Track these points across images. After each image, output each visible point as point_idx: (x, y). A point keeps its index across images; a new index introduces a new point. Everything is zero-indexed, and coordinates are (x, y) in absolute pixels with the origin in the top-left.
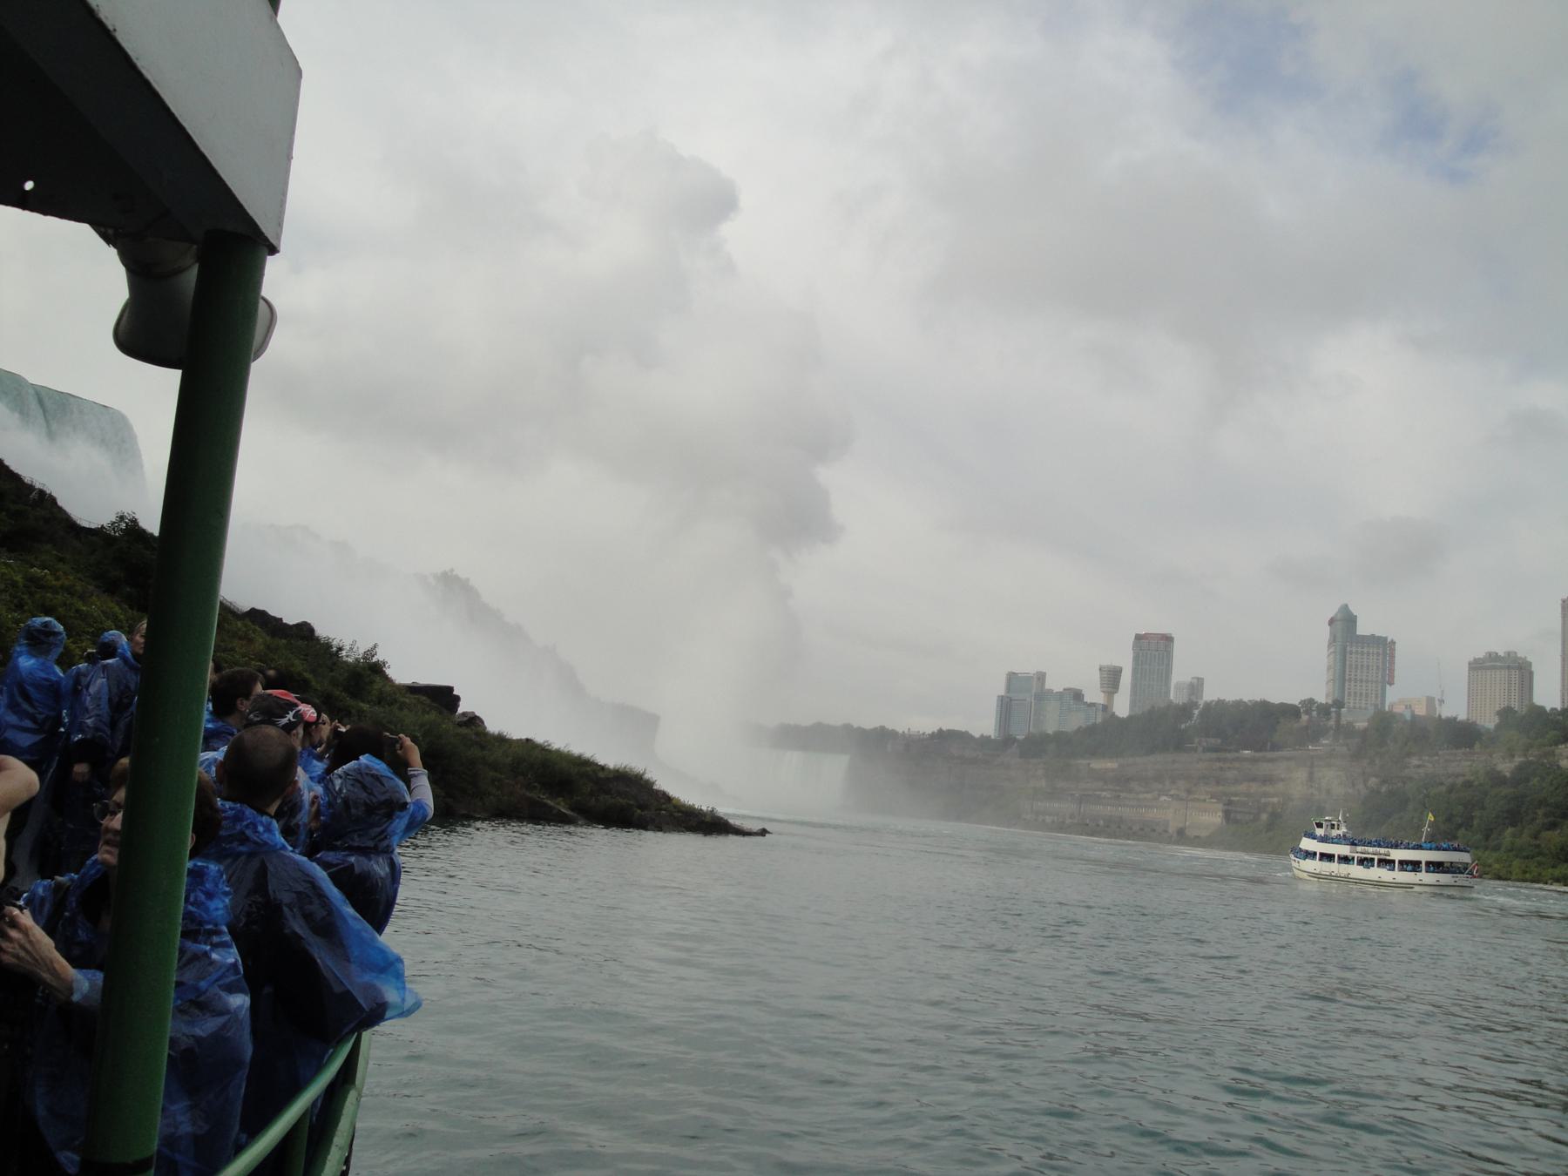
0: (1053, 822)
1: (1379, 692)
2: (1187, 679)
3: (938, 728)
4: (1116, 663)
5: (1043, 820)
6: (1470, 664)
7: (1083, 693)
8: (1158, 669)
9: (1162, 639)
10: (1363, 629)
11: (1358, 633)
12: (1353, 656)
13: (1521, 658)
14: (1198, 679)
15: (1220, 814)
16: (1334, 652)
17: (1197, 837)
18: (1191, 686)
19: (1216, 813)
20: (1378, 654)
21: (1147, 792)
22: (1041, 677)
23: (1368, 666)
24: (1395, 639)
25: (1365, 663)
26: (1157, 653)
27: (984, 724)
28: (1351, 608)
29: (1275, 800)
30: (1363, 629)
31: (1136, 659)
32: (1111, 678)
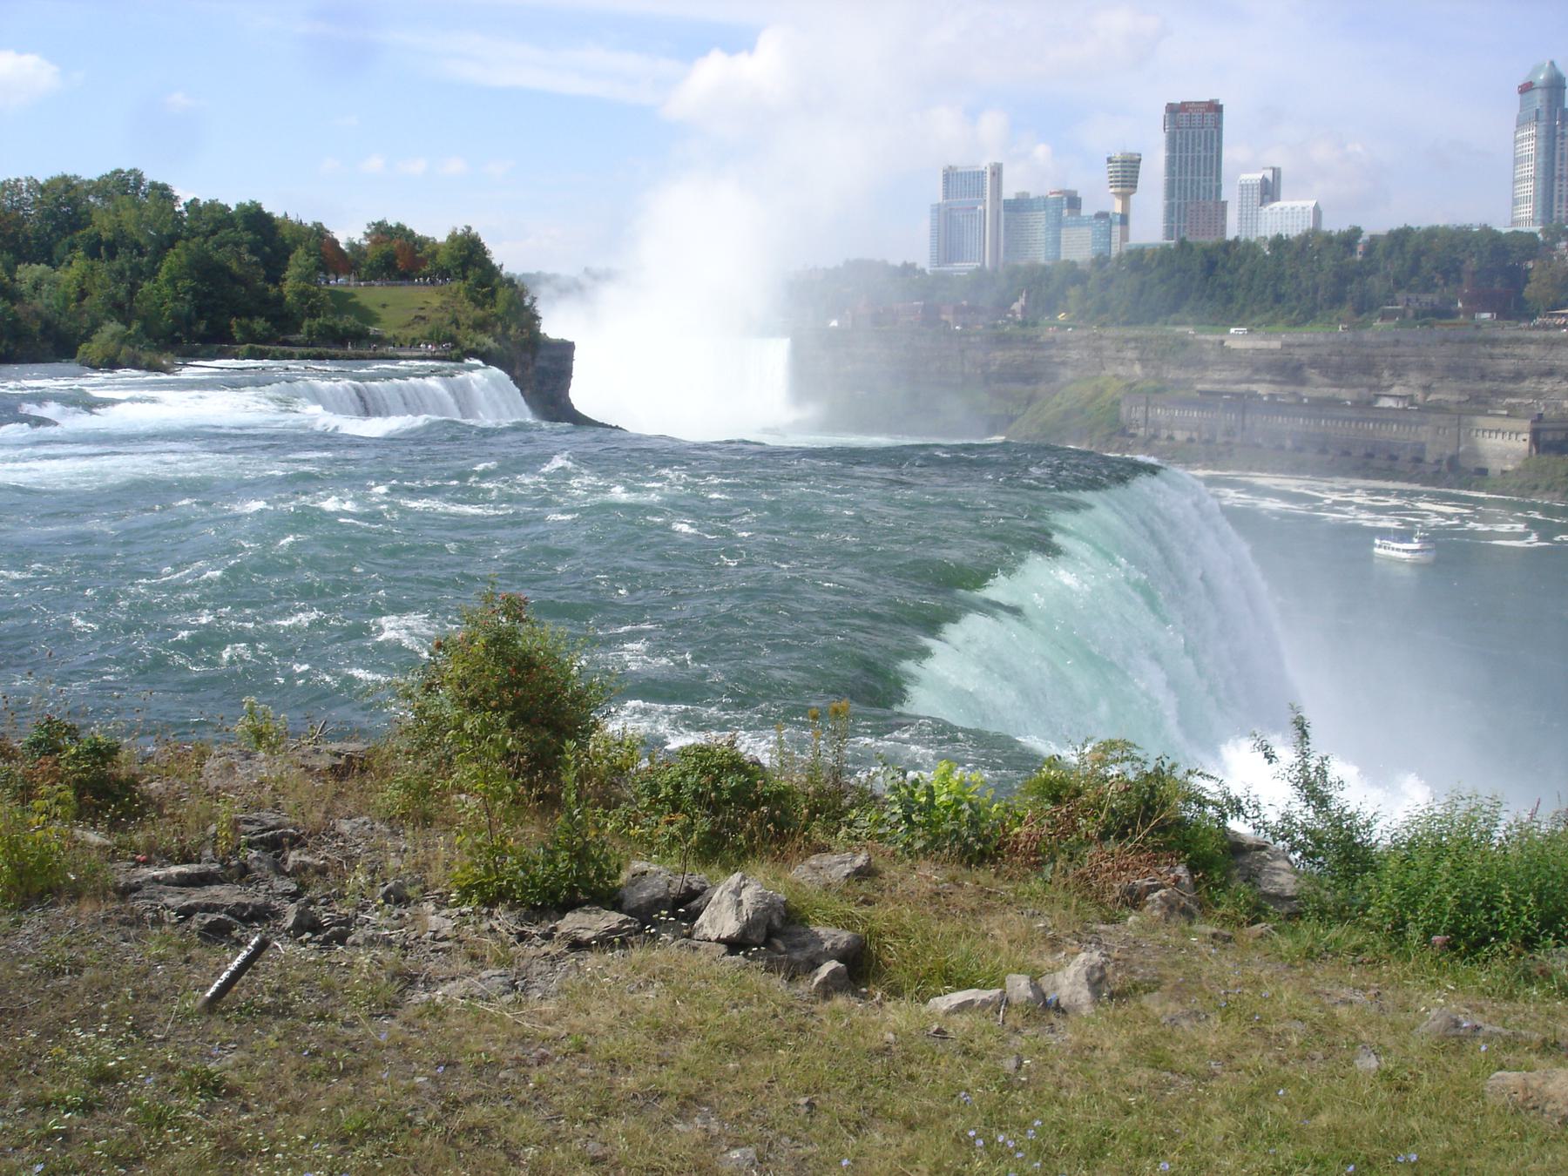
0: (1190, 440)
5: (1170, 438)
8: (1205, 157)
14: (1274, 169)
15: (1527, 436)
18: (1264, 181)
19: (1517, 434)
21: (1342, 387)
22: (997, 172)
26: (1203, 131)
31: (1172, 144)
32: (1127, 173)
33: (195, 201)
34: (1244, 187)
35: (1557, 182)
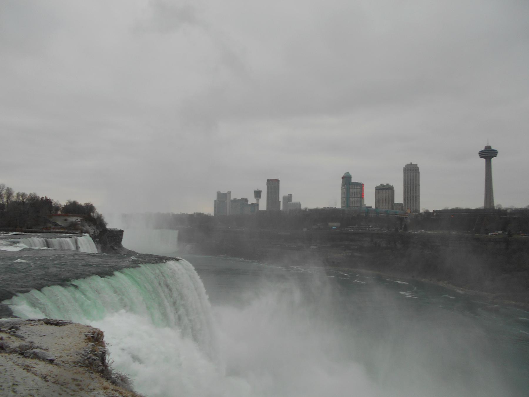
1: (360, 201)
2: (286, 194)
3: (194, 212)
4: (260, 189)
6: (376, 188)
7: (248, 199)
9: (276, 181)
10: (353, 180)
11: (352, 182)
12: (352, 189)
13: (391, 186)
14: (290, 194)
16: (344, 188)
17: (333, 262)
20: (359, 188)
22: (229, 193)
23: (356, 192)
24: (364, 184)
25: (355, 192)
27: (209, 209)
28: (349, 173)
29: (356, 247)
30: (353, 180)
31: (268, 188)
32: (258, 194)
33: (19, 192)
34: (284, 198)
35: (350, 199)
